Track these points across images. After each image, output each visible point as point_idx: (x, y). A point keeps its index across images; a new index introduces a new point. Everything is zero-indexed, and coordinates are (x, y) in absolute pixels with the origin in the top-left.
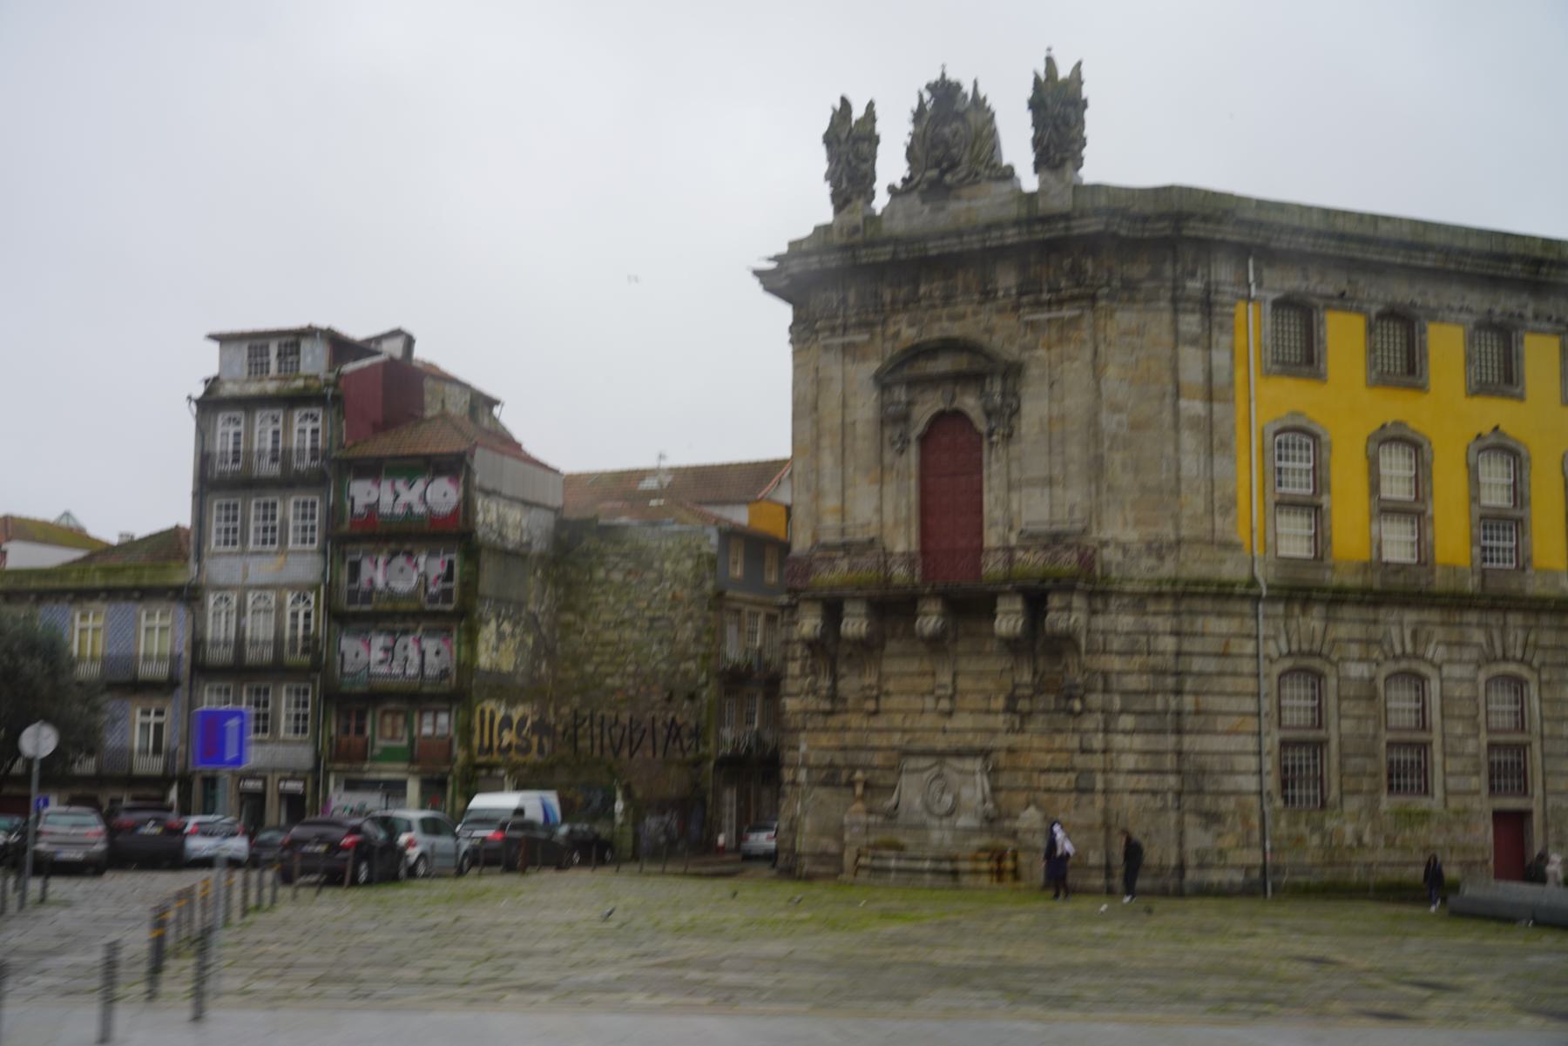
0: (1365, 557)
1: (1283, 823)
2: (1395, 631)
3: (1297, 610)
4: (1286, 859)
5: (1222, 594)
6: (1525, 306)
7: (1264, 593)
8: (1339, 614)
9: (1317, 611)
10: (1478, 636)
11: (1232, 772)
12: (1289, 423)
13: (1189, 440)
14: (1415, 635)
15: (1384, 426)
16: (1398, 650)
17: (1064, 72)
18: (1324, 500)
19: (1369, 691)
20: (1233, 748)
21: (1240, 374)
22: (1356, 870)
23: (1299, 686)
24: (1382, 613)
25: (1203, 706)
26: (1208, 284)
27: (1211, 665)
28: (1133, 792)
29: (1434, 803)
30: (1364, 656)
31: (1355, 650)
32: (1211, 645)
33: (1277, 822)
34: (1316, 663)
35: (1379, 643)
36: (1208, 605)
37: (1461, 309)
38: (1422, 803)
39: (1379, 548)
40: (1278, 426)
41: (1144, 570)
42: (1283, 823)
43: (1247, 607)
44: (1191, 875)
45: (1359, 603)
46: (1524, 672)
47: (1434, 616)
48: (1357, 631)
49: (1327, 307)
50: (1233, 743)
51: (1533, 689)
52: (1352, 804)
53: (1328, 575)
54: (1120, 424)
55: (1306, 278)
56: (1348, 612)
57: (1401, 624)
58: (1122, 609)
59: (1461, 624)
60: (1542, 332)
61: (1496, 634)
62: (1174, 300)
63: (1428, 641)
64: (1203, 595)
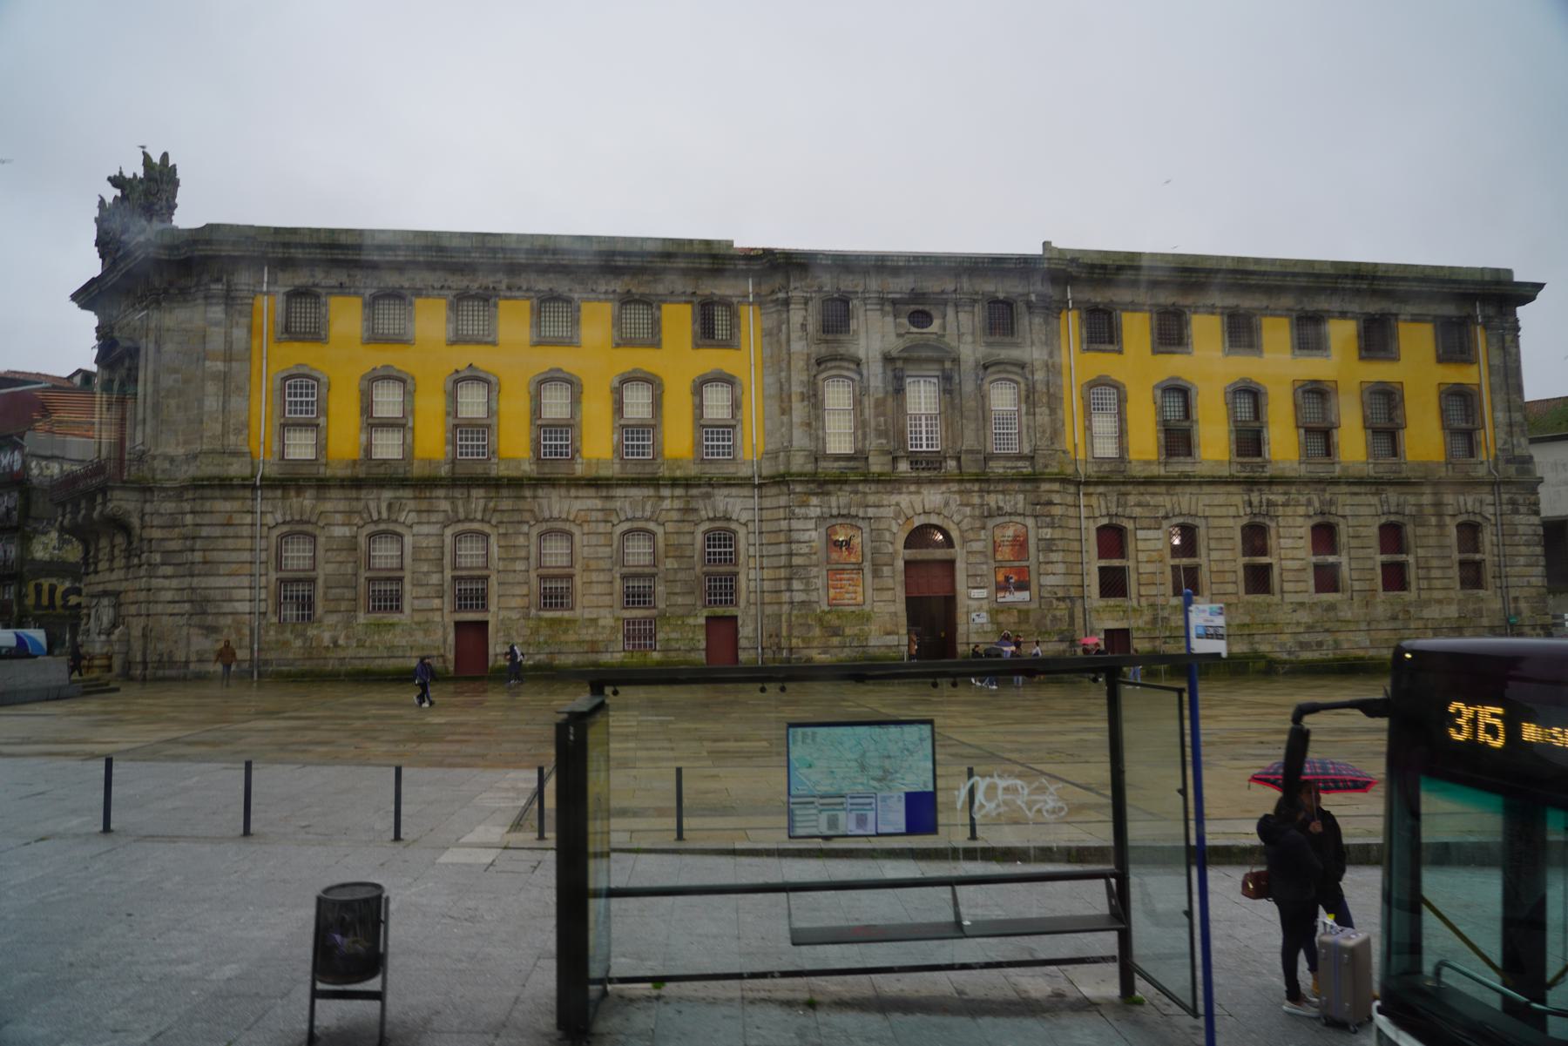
0: (356, 457)
1: (272, 633)
2: (372, 505)
3: (292, 493)
4: (271, 655)
5: (224, 485)
6: (500, 282)
7: (258, 483)
8: (328, 495)
9: (309, 493)
10: (445, 505)
11: (231, 600)
12: (295, 371)
13: (211, 387)
14: (390, 506)
15: (374, 369)
16: (375, 517)
17: (156, 159)
18: (322, 421)
19: (352, 545)
20: (232, 585)
21: (256, 344)
22: (331, 662)
23: (304, 543)
24: (363, 493)
25: (209, 559)
26: (229, 285)
27: (217, 532)
28: (171, 615)
29: (404, 617)
30: (347, 522)
31: (339, 518)
32: (217, 519)
33: (267, 632)
34: (308, 528)
35: (359, 512)
36: (217, 493)
37: (442, 287)
38: (394, 617)
39: (368, 449)
40: (285, 374)
41: (187, 472)
42: (272, 633)
43: (248, 493)
44: (192, 666)
45: (342, 487)
46: (486, 528)
47: (408, 493)
48: (342, 506)
49: (328, 294)
50: (231, 582)
51: (493, 540)
52: (332, 619)
53: (322, 470)
54: (176, 381)
55: (313, 276)
56: (334, 493)
57: (379, 499)
58: (164, 500)
59: (430, 498)
60: (515, 298)
61: (460, 503)
62: (206, 298)
63: (400, 510)
64: (211, 487)
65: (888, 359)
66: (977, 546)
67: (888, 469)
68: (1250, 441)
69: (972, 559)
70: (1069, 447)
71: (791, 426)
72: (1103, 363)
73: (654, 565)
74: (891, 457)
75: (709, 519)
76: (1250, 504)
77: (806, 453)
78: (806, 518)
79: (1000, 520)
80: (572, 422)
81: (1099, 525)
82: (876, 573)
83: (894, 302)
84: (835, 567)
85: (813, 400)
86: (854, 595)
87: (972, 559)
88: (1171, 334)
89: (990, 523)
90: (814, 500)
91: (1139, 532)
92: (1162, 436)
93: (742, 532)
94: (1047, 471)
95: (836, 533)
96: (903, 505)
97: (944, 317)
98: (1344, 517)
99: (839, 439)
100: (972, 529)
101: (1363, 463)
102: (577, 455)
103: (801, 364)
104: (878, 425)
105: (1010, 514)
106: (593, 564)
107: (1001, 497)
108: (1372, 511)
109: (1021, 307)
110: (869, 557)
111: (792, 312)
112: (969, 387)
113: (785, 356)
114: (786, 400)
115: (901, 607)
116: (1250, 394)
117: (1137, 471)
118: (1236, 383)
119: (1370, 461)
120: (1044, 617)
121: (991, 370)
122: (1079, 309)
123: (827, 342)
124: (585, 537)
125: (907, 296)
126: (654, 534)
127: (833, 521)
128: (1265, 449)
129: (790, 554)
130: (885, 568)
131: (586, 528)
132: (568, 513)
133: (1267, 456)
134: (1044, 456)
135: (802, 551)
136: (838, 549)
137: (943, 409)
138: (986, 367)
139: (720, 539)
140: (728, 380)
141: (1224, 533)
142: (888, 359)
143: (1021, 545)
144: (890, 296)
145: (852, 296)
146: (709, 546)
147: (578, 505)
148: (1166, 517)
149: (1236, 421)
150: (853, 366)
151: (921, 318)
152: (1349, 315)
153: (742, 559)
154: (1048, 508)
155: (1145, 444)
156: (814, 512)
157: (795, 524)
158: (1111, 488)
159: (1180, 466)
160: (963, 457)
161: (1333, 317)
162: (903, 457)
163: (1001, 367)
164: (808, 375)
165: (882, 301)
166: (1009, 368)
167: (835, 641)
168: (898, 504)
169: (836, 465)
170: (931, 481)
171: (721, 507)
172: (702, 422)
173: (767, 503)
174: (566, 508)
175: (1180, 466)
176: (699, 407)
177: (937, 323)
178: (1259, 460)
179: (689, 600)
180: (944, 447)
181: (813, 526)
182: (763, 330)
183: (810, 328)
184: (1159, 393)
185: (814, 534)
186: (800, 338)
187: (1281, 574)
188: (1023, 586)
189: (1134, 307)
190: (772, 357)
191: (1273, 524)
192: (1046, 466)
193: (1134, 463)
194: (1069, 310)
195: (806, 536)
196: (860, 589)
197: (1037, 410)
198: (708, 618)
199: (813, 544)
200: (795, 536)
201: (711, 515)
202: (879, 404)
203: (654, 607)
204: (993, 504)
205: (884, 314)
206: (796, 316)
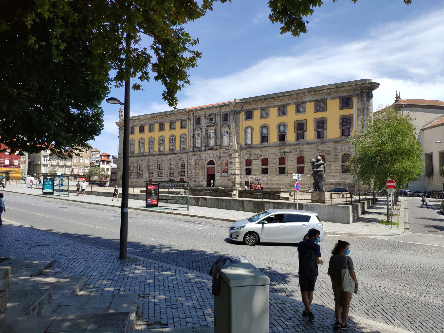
66: (218, 164)
68: (282, 138)
69: (217, 167)
70: (241, 143)
72: (249, 123)
76: (280, 152)
88: (264, 115)
90: (193, 157)
96: (206, 157)
97: (215, 118)
99: (199, 145)
103: (193, 131)
116: (264, 128)
117: (255, 146)
118: (279, 124)
141: (274, 160)
149: (279, 132)
151: (211, 119)
155: (257, 140)
156: (193, 159)
175: (265, 144)
177: (214, 120)
183: (194, 124)
188: (226, 172)
189: (257, 109)
202: (204, 137)
204: (221, 156)
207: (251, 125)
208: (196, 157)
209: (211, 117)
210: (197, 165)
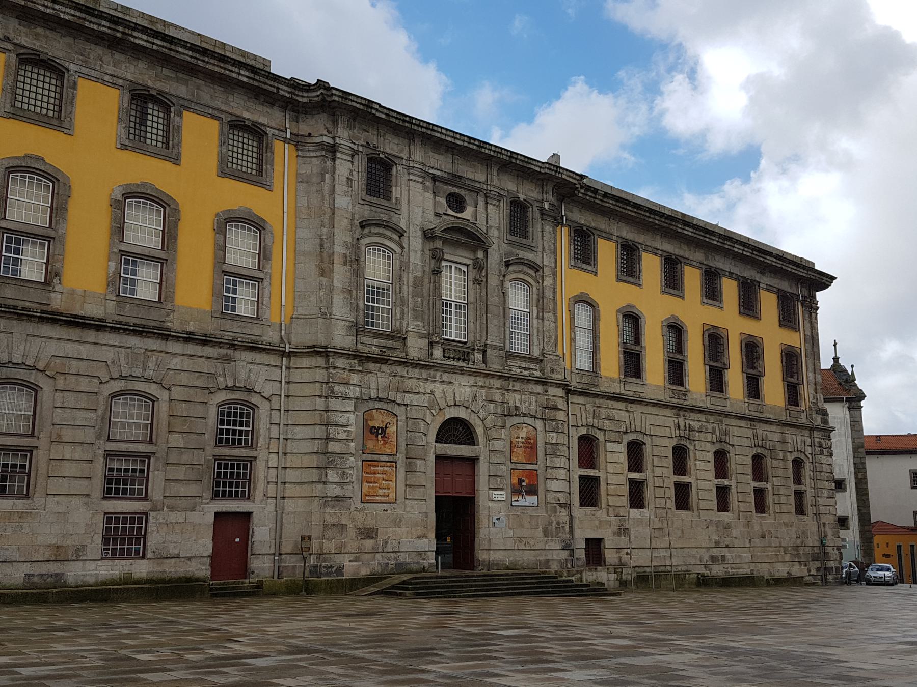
65: (428, 235)
66: (498, 445)
67: (423, 355)
69: (494, 459)
71: (332, 290)
73: (151, 442)
74: (427, 341)
75: (227, 388)
77: (347, 323)
78: (344, 398)
79: (516, 420)
80: (52, 233)
81: (580, 434)
82: (410, 470)
83: (434, 179)
84: (369, 457)
85: (355, 266)
86: (386, 491)
87: (494, 459)
89: (510, 421)
90: (355, 378)
91: (608, 444)
92: (622, 356)
93: (264, 407)
94: (553, 376)
95: (372, 419)
96: (437, 395)
98: (733, 446)
100: (494, 427)
101: (741, 401)
102: (56, 281)
104: (415, 305)
105: (525, 415)
106: (68, 434)
107: (517, 397)
108: (747, 442)
109: (534, 213)
110: (403, 448)
111: (338, 162)
112: (494, 281)
113: (328, 211)
114: (326, 259)
115: (430, 505)
119: (746, 400)
120: (550, 523)
121: (511, 268)
122: (569, 226)
123: (371, 204)
124: (58, 394)
125: (445, 175)
126: (153, 400)
127: (371, 405)
128: (686, 379)
129: (328, 439)
130: (418, 462)
131: (61, 383)
132: (37, 359)
133: (687, 387)
134: (552, 361)
135: (339, 437)
136: (373, 436)
137: (472, 299)
138: (508, 264)
139: (235, 415)
140: (256, 224)
142: (428, 235)
143: (531, 448)
144: (432, 171)
145: (397, 161)
146: (222, 423)
147: (52, 348)
148: (625, 433)
150: (396, 237)
152: (734, 276)
153: (261, 442)
154: (554, 412)
156: (354, 392)
157: (334, 404)
158: (589, 399)
159: (632, 388)
160: (489, 351)
161: (724, 275)
162: (438, 343)
163: (521, 267)
164: (353, 238)
165: (425, 174)
166: (526, 269)
167: (369, 543)
168: (432, 393)
169: (375, 341)
170: (461, 371)
171: (243, 375)
172: (225, 267)
173: (296, 376)
174: (34, 351)
176: (221, 249)
178: (681, 388)
179: (193, 489)
180: (472, 339)
181: (352, 409)
182: (298, 174)
184: (621, 316)
185: (352, 417)
186: (346, 194)
187: (698, 493)
188: (532, 490)
190: (308, 207)
191: (691, 448)
192: (552, 371)
193: (604, 379)
194: (563, 225)
195: (342, 420)
196: (392, 485)
197: (545, 315)
198: (217, 515)
199: (349, 428)
200: (334, 417)
201: (230, 384)
202: (418, 283)
203: (146, 498)
204: (511, 403)
205: (425, 189)
206: (343, 167)
207: (595, 296)
208: (373, 386)
209: (457, 190)
210: (379, 432)
